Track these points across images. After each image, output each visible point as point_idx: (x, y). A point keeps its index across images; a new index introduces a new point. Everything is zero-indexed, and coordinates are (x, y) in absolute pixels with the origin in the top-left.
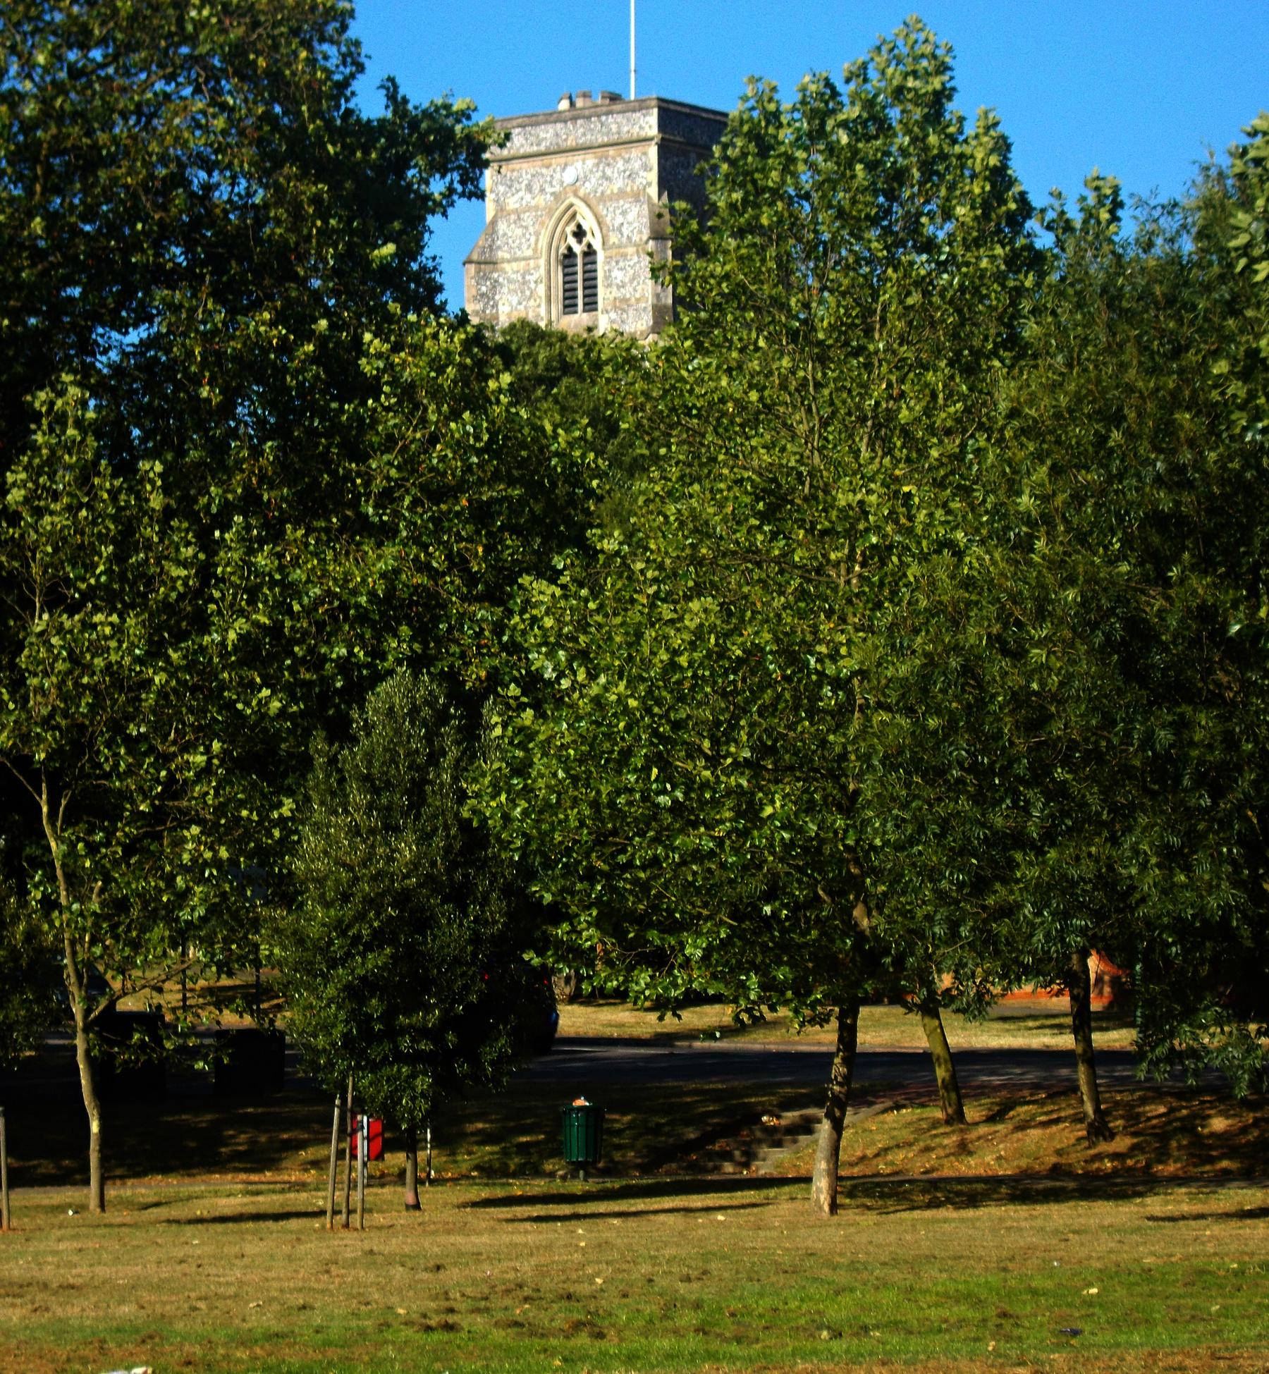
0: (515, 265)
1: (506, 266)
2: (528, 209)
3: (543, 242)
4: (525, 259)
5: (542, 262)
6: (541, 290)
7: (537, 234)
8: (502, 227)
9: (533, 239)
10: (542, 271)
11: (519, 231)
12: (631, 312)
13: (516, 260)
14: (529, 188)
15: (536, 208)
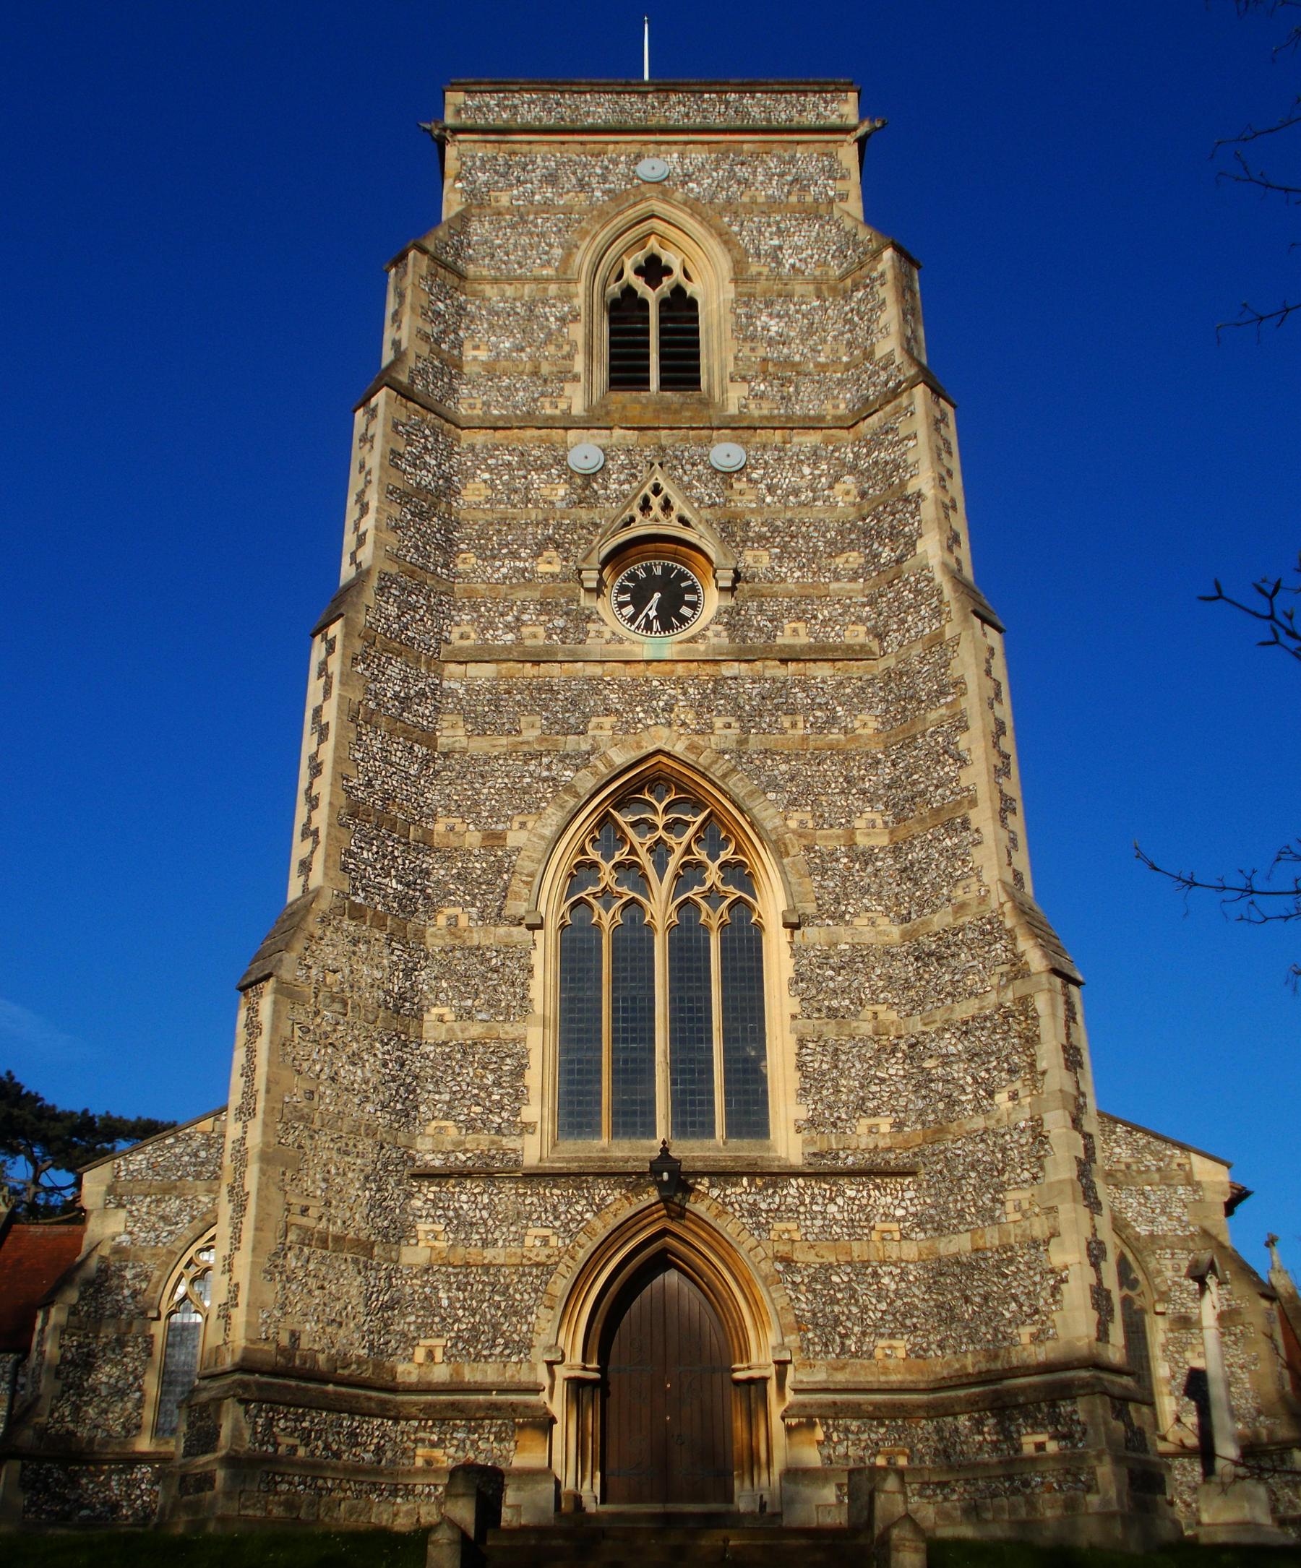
0: (510, 291)
1: (490, 291)
2: (547, 206)
3: (583, 259)
4: (537, 280)
5: (581, 288)
6: (577, 332)
7: (569, 250)
8: (479, 229)
9: (557, 252)
10: (580, 302)
11: (525, 240)
12: (807, 388)
13: (510, 280)
14: (551, 179)
15: (568, 210)
